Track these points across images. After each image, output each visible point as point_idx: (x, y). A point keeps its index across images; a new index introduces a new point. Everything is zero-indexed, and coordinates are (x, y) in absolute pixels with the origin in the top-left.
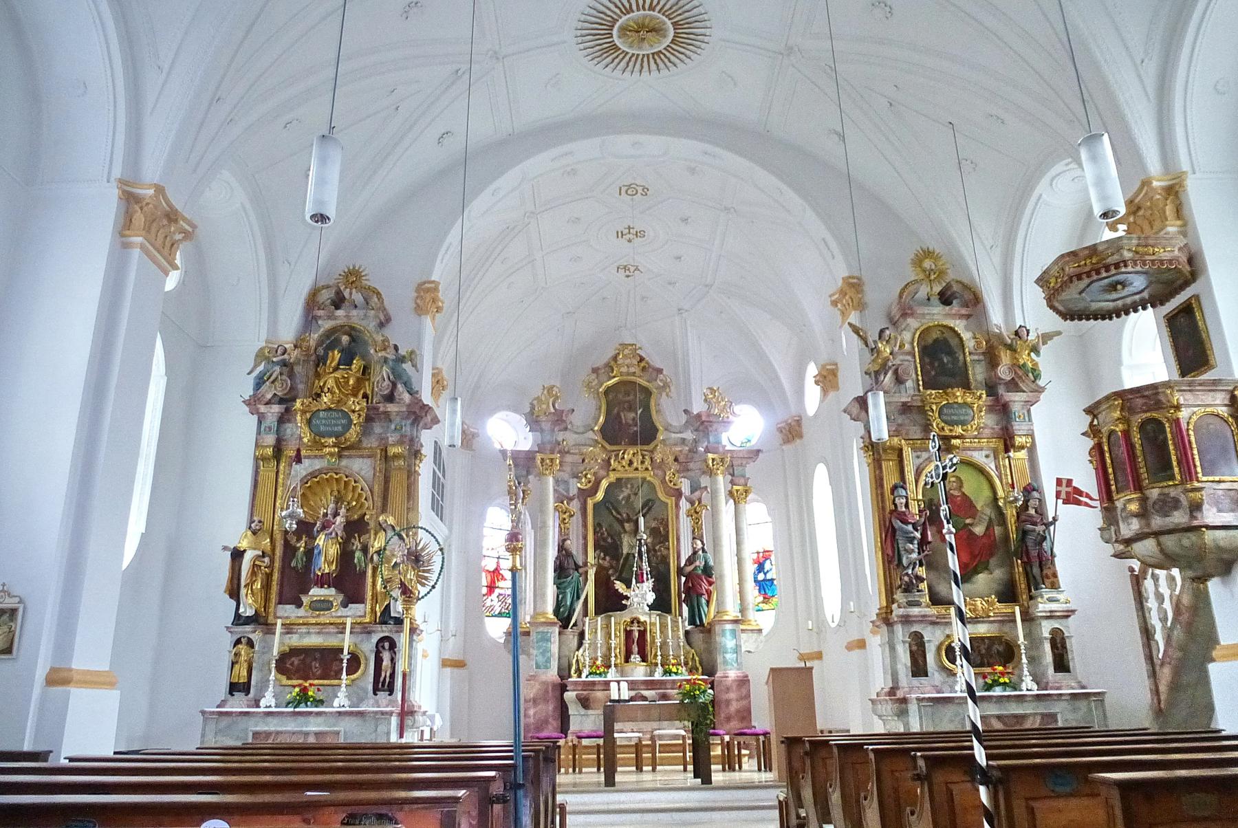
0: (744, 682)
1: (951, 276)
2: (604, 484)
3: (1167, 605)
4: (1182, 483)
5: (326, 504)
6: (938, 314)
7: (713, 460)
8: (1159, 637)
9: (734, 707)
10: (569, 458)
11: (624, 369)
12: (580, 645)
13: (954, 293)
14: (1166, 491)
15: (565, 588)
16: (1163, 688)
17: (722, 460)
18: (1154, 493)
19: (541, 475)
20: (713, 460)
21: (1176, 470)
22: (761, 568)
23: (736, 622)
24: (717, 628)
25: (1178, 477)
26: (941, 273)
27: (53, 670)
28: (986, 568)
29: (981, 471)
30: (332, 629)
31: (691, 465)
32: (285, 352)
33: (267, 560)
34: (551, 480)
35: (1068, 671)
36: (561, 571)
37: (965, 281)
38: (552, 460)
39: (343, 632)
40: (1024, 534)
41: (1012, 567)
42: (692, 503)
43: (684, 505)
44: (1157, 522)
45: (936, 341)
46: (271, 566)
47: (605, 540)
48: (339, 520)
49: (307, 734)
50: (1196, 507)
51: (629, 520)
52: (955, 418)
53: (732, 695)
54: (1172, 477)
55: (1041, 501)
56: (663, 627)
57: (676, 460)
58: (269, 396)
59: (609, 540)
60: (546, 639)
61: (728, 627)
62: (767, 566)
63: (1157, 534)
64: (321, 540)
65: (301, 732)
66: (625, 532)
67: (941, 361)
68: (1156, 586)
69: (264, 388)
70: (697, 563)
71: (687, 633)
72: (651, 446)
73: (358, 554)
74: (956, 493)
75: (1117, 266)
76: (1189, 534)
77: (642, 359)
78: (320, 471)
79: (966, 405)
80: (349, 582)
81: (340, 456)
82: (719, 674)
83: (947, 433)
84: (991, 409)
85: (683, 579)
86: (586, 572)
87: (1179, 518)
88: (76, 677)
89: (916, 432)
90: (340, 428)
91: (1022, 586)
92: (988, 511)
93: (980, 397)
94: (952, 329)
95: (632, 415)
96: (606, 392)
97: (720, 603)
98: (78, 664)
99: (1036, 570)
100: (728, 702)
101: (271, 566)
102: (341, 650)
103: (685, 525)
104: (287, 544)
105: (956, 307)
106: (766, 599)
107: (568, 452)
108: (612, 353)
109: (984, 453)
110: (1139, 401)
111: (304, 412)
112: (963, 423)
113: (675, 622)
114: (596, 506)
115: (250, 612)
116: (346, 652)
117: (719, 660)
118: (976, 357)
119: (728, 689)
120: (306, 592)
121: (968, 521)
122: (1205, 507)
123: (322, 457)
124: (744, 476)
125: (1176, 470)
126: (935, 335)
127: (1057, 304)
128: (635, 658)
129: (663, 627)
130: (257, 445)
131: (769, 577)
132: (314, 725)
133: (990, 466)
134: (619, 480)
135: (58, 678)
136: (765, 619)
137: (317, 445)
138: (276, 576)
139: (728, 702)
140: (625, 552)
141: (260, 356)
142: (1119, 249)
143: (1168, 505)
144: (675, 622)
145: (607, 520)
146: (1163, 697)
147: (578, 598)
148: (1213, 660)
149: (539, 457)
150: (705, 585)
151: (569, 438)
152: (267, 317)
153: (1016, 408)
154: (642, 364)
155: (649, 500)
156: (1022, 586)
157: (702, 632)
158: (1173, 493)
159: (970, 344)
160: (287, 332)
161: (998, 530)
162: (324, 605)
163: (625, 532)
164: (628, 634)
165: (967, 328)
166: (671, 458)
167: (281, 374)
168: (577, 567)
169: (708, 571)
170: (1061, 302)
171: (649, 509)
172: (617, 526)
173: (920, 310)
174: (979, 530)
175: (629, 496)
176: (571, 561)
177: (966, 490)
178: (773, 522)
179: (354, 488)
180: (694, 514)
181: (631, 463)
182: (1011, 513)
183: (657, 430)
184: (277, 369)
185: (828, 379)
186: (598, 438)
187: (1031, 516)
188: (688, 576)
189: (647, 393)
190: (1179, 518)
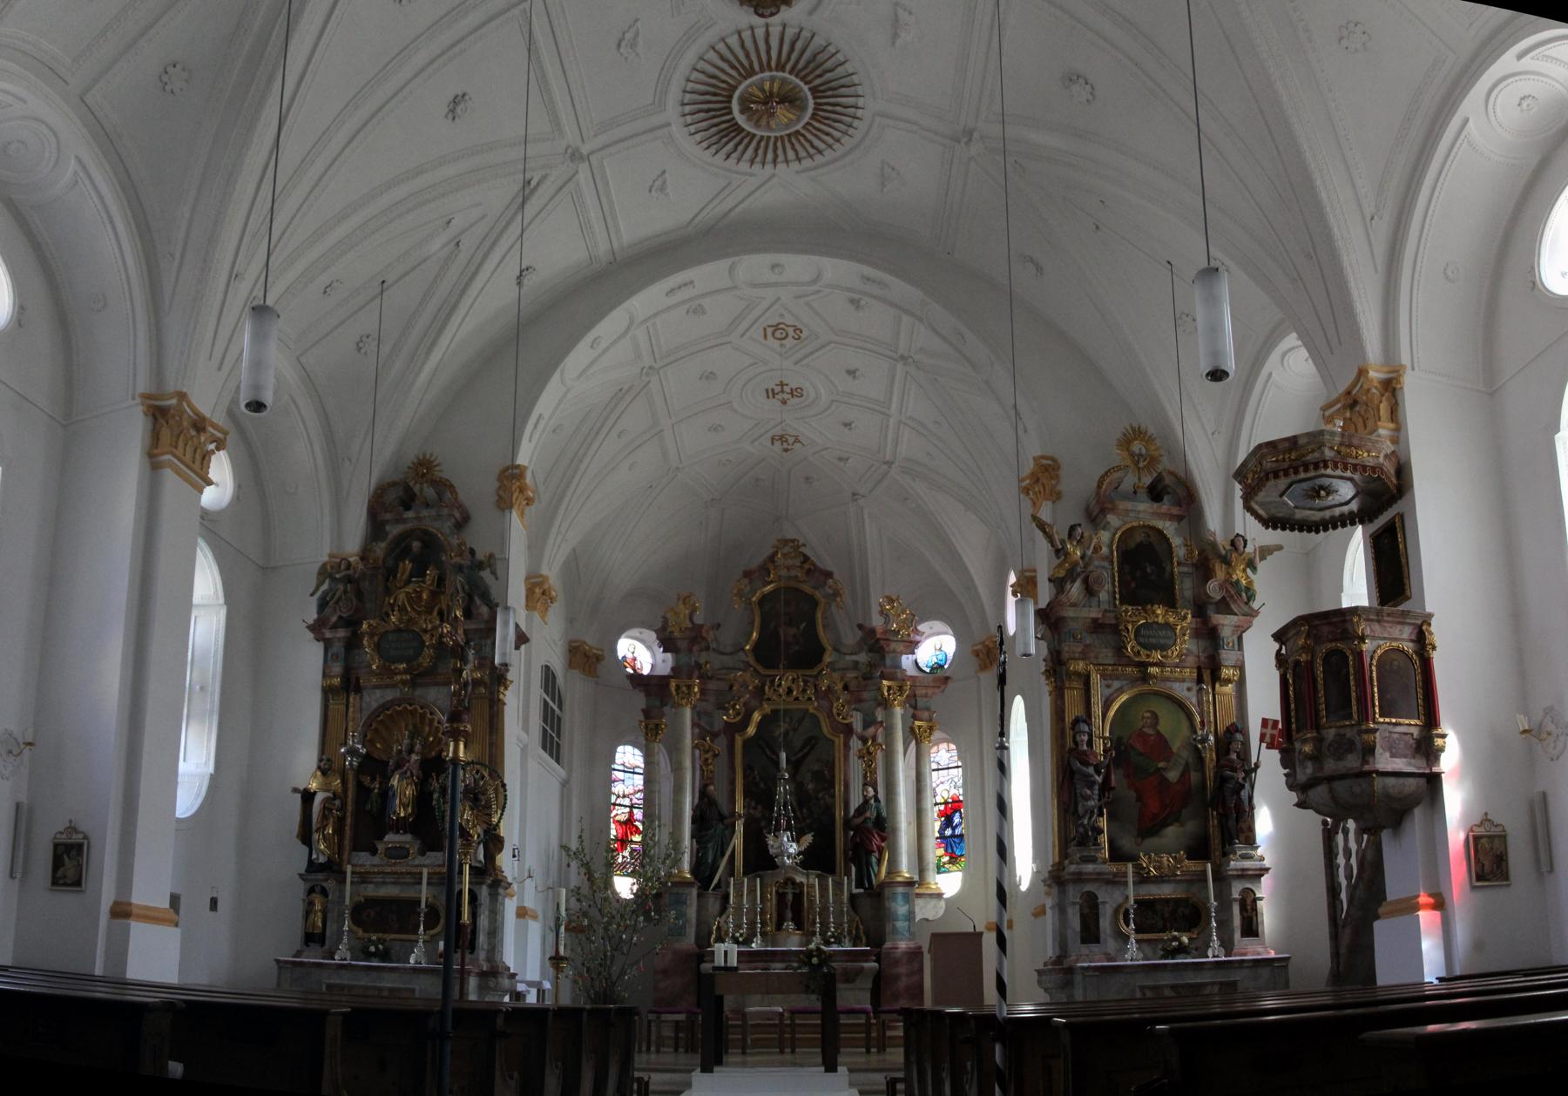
0: (916, 954)
1: (1165, 464)
2: (756, 717)
3: (1353, 861)
4: (1359, 723)
5: (401, 740)
6: (1144, 512)
7: (889, 688)
8: (1343, 896)
9: (903, 983)
10: (712, 685)
11: (784, 573)
12: (723, 909)
13: (1166, 486)
14: (1342, 731)
16: (1343, 950)
17: (901, 688)
18: (1330, 734)
19: (678, 706)
20: (889, 688)
21: (1355, 708)
22: (948, 822)
24: (887, 891)
25: (1355, 716)
26: (1153, 461)
27: (116, 904)
28: (1177, 820)
29: (1181, 705)
30: (408, 879)
31: (866, 695)
32: (349, 565)
33: (337, 802)
34: (688, 713)
35: (1256, 935)
36: (701, 820)
37: (1182, 474)
38: (689, 687)
39: (420, 883)
40: (1222, 780)
41: (1207, 819)
42: (864, 740)
43: (855, 744)
44: (1330, 766)
45: (1140, 545)
46: (343, 808)
48: (414, 757)
49: (380, 989)
50: (1370, 750)
52: (1153, 641)
53: (902, 970)
54: (1350, 717)
55: (1246, 744)
56: (824, 889)
57: (846, 687)
58: (334, 619)
60: (680, 902)
61: (900, 890)
62: (956, 820)
63: (1330, 779)
64: (395, 782)
65: (374, 988)
67: (1145, 571)
68: (1346, 840)
69: (328, 610)
71: (852, 897)
72: (815, 672)
73: (436, 796)
74: (1150, 731)
75: (1316, 467)
76: (1360, 780)
77: (806, 559)
78: (392, 703)
79: (1167, 625)
80: (428, 826)
81: (413, 684)
82: (888, 945)
83: (1143, 658)
84: (1197, 634)
87: (1352, 762)
88: (135, 911)
89: (1107, 656)
90: (411, 652)
91: (1216, 841)
92: (1185, 754)
93: (1185, 618)
94: (1160, 532)
95: (793, 631)
96: (761, 602)
97: (894, 863)
98: (138, 898)
99: (1232, 823)
100: (897, 977)
101: (343, 808)
102: (419, 902)
103: (856, 768)
104: (360, 785)
105: (1165, 506)
106: (954, 859)
107: (711, 678)
108: (772, 551)
109: (1186, 685)
110: (1326, 629)
111: (371, 635)
112: (1163, 648)
113: (838, 885)
115: (322, 859)
116: (423, 905)
117: (888, 928)
118: (1185, 569)
119: (896, 962)
120: (381, 838)
121: (1161, 765)
122: (1378, 750)
123: (394, 686)
124: (928, 709)
125: (1355, 708)
126: (1139, 537)
127: (1256, 507)
128: (790, 925)
129: (824, 889)
130: (325, 675)
131: (957, 832)
132: (388, 982)
133: (1191, 699)
134: (775, 712)
135: (122, 911)
136: (949, 883)
137: (386, 671)
138: (349, 820)
139: (897, 977)
141: (324, 573)
142: (1321, 446)
143: (1343, 747)
144: (838, 885)
146: (1342, 960)
147: (723, 855)
148: (1378, 917)
149: (673, 684)
150: (876, 841)
151: (713, 661)
152: (332, 529)
153: (1226, 632)
154: (806, 566)
155: (810, 739)
156: (1216, 841)
158: (1349, 733)
159: (1180, 553)
160: (352, 544)
161: (1194, 777)
162: (399, 853)
164: (781, 897)
165: (1178, 532)
166: (839, 686)
167: (345, 592)
168: (722, 818)
170: (1261, 505)
171: (812, 748)
173: (1123, 505)
174: (1173, 775)
175: (786, 734)
177: (1161, 728)
178: (964, 767)
179: (432, 721)
181: (790, 691)
182: (1210, 757)
183: (822, 650)
184: (341, 587)
185: (1026, 587)
186: (751, 660)
187: (1232, 761)
189: (814, 603)
190: (1352, 762)
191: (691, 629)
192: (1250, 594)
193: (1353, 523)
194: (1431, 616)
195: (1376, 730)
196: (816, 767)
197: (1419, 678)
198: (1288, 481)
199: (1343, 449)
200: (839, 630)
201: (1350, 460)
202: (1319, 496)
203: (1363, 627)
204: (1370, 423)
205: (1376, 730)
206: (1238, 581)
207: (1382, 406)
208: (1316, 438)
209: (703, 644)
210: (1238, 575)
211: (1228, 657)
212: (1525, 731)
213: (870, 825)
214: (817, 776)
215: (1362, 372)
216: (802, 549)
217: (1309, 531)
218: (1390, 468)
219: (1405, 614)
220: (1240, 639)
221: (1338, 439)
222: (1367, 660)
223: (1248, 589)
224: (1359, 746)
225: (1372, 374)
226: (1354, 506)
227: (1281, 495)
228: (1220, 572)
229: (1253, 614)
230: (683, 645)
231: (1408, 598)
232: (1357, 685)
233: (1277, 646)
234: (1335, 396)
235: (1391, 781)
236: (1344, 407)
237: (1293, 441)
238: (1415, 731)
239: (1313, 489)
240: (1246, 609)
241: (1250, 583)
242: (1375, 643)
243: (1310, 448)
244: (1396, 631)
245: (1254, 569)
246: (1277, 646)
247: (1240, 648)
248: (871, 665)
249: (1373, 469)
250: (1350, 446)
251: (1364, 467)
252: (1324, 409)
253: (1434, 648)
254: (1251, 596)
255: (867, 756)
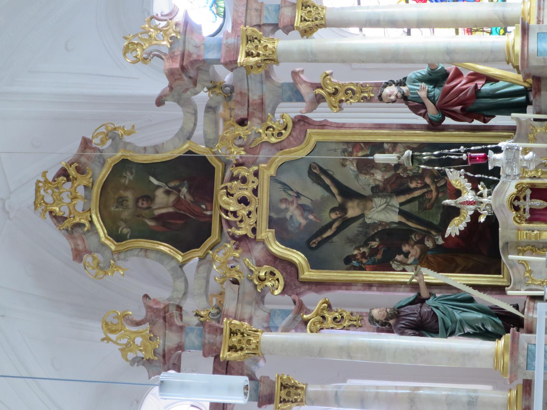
2: (277, 249)
10: (230, 306)
11: (79, 205)
15: (454, 321)
17: (250, 39)
23: (525, 30)
31: (254, 97)
34: (267, 337)
36: (425, 326)
38: (233, 333)
42: (319, 99)
43: (320, 114)
47: (374, 252)
51: (342, 208)
57: (242, 122)
59: (375, 244)
61: (533, 44)
66: (362, 216)
70: (423, 94)
72: (218, 166)
77: (64, 173)
85: (448, 121)
86: (429, 285)
95: (160, 195)
96: (118, 238)
97: (491, 56)
114: (314, 265)
124: (279, 8)
134: (272, 223)
140: (395, 218)
145: (341, 246)
147: (471, 300)
154: (72, 172)
155: (310, 173)
157: (538, 91)
163: (362, 216)
166: (241, 131)
168: (419, 300)
169: (436, 78)
171: (324, 172)
172: (354, 228)
175: (303, 208)
176: (407, 310)
180: (339, 96)
181: (244, 201)
186: (195, 255)
188: (445, 110)
191: (153, 323)
196: (352, 167)
200: (160, 135)
209: (173, 310)
213: (437, 92)
214: (366, 166)
216: (50, 177)
230: (173, 339)
248: (214, 86)
255: (339, 96)
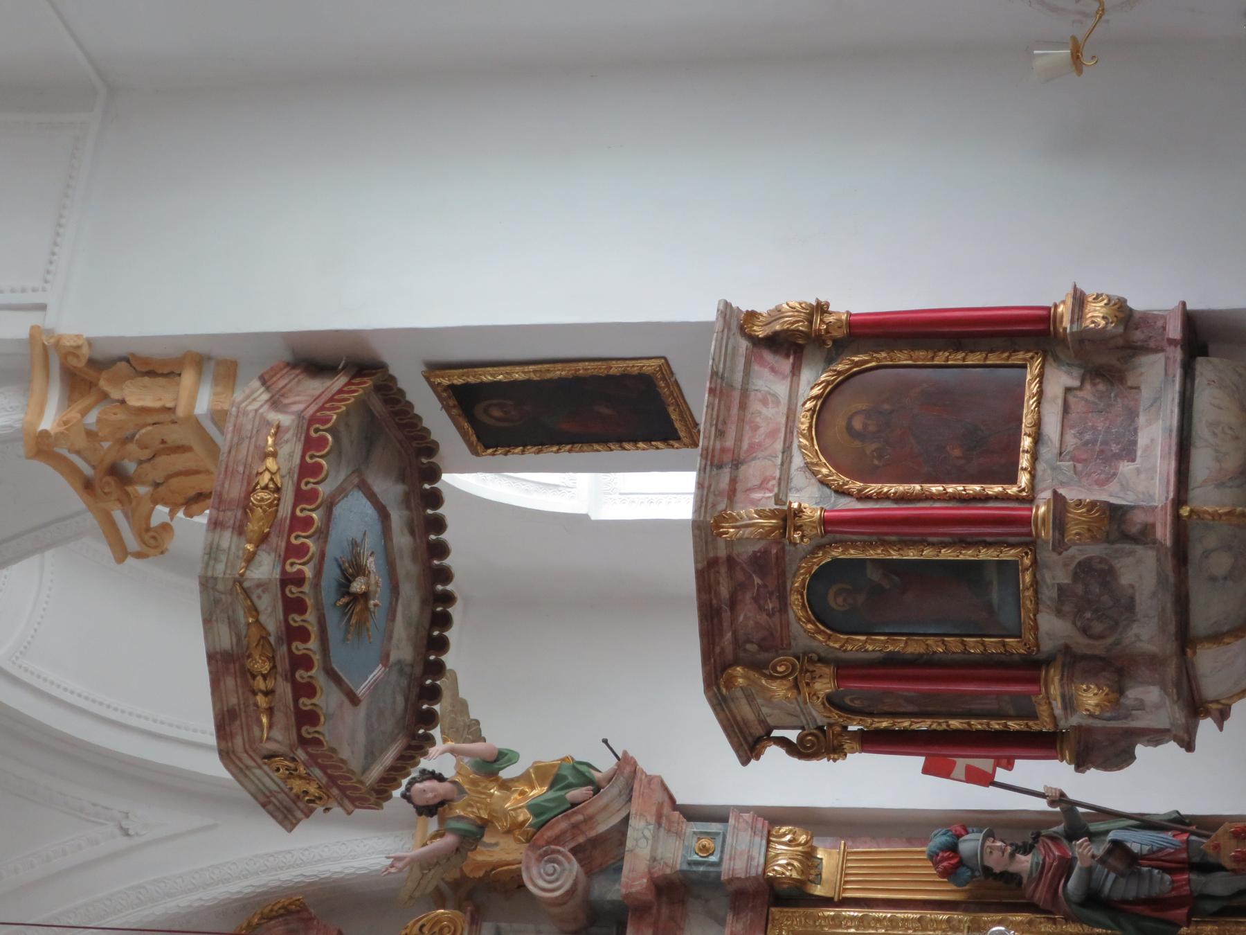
4: (1030, 544)
14: (1049, 594)
18: (1053, 628)
21: (985, 554)
25: (1009, 554)
44: (1146, 634)
50: (1114, 522)
54: (1008, 570)
55: (992, 824)
63: (1185, 640)
76: (1196, 551)
87: (1140, 573)
110: (748, 616)
122: (1111, 495)
125: (985, 554)
127: (376, 771)
143: (1094, 592)
153: (675, 852)
158: (1058, 574)
170: (372, 755)
187: (1042, 869)
190: (1140, 573)
192: (569, 776)
193: (435, 499)
194: (727, 310)
195: (1058, 499)
197: (902, 358)
198: (321, 680)
199: (253, 527)
201: (285, 509)
202: (365, 596)
203: (752, 511)
204: (175, 435)
205: (1058, 499)
206: (537, 809)
207: (134, 402)
208: (221, 598)
210: (517, 805)
211: (742, 855)
212: (1076, 57)
215: (43, 448)
217: (444, 621)
218: (309, 392)
219: (720, 388)
220: (693, 814)
221: (226, 539)
222: (847, 506)
223: (557, 781)
224: (1095, 550)
225: (48, 423)
226: (389, 490)
227: (354, 700)
228: (500, 850)
229: (627, 766)
231: (666, 367)
232: (923, 542)
233: (773, 753)
234: (90, 520)
235: (1202, 463)
236: (126, 500)
237: (223, 664)
238: (1060, 380)
239: (346, 610)
240: (610, 793)
241: (541, 773)
242: (799, 478)
243: (242, 618)
244: (768, 416)
245: (502, 758)
246: (773, 753)
247: (718, 815)
249: (310, 444)
250: (246, 507)
251: (307, 470)
252: (121, 553)
253: (821, 308)
254: (581, 775)
